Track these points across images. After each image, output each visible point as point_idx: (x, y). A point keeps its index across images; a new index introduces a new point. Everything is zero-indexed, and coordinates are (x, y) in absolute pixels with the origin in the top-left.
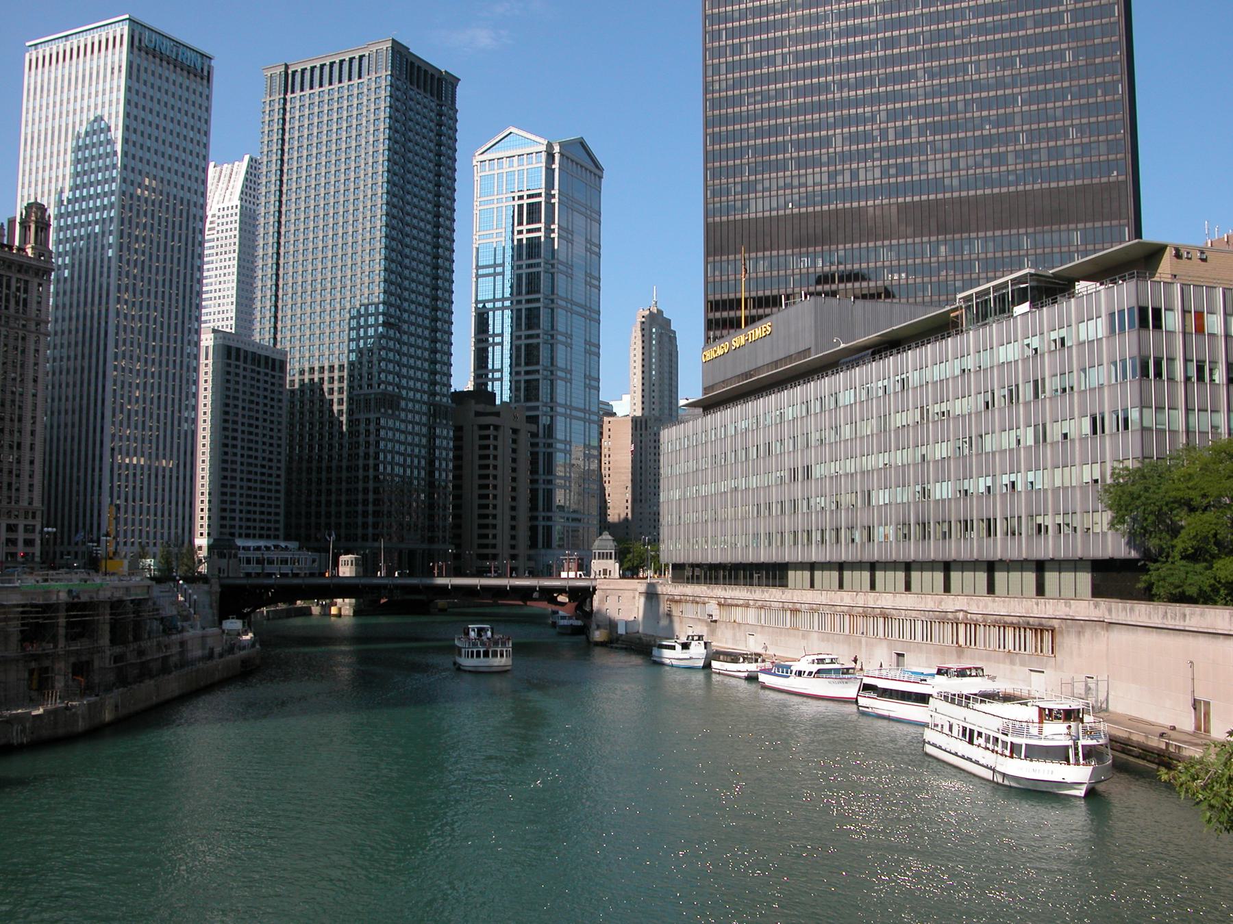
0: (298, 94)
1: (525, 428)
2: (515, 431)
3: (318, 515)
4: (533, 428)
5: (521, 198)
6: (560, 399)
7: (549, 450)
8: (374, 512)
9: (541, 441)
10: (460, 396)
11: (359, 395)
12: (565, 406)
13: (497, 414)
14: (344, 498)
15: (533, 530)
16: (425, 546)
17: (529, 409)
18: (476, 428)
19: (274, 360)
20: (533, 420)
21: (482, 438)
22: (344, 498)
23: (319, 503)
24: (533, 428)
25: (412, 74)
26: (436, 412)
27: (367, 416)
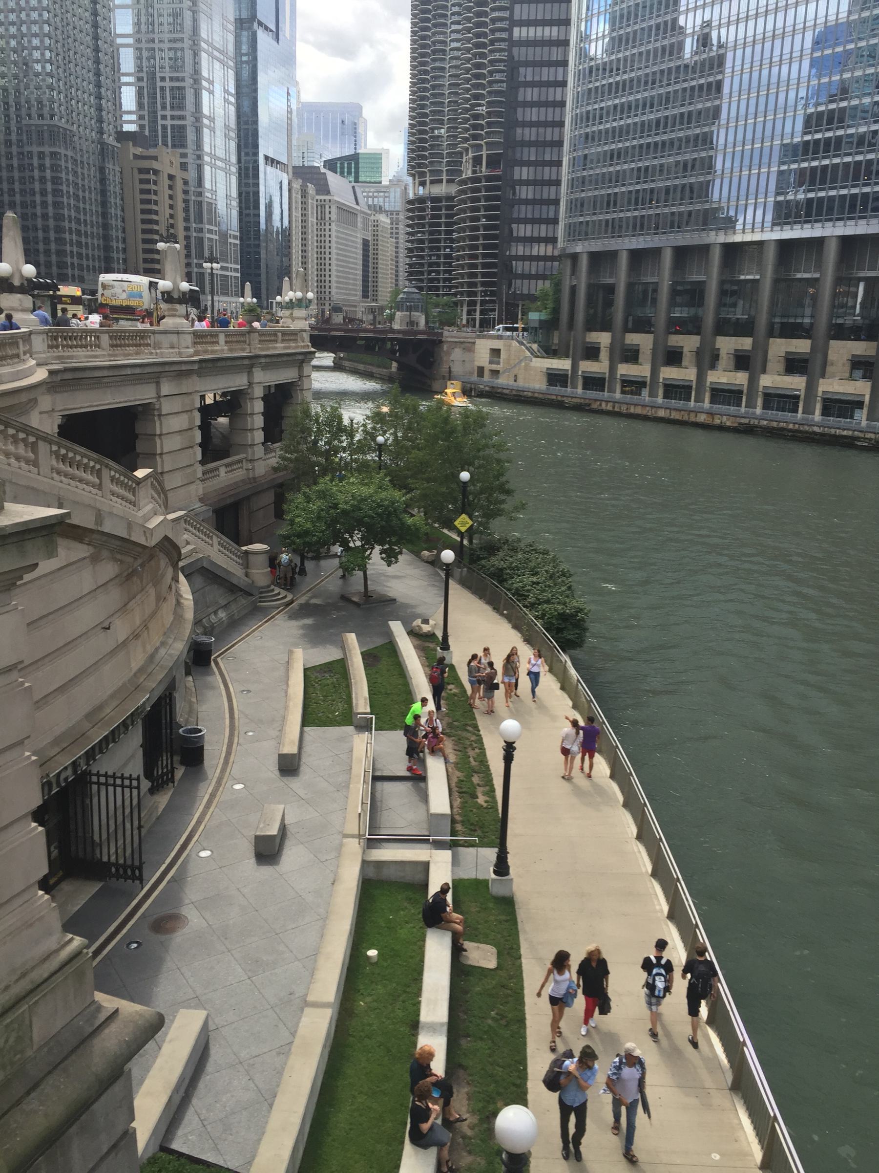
2: (171, 177)
4: (184, 175)
6: (207, 148)
7: (199, 199)
10: (123, 136)
18: (136, 171)
20: (184, 167)
21: (142, 181)
26: (104, 151)
27: (42, 149)
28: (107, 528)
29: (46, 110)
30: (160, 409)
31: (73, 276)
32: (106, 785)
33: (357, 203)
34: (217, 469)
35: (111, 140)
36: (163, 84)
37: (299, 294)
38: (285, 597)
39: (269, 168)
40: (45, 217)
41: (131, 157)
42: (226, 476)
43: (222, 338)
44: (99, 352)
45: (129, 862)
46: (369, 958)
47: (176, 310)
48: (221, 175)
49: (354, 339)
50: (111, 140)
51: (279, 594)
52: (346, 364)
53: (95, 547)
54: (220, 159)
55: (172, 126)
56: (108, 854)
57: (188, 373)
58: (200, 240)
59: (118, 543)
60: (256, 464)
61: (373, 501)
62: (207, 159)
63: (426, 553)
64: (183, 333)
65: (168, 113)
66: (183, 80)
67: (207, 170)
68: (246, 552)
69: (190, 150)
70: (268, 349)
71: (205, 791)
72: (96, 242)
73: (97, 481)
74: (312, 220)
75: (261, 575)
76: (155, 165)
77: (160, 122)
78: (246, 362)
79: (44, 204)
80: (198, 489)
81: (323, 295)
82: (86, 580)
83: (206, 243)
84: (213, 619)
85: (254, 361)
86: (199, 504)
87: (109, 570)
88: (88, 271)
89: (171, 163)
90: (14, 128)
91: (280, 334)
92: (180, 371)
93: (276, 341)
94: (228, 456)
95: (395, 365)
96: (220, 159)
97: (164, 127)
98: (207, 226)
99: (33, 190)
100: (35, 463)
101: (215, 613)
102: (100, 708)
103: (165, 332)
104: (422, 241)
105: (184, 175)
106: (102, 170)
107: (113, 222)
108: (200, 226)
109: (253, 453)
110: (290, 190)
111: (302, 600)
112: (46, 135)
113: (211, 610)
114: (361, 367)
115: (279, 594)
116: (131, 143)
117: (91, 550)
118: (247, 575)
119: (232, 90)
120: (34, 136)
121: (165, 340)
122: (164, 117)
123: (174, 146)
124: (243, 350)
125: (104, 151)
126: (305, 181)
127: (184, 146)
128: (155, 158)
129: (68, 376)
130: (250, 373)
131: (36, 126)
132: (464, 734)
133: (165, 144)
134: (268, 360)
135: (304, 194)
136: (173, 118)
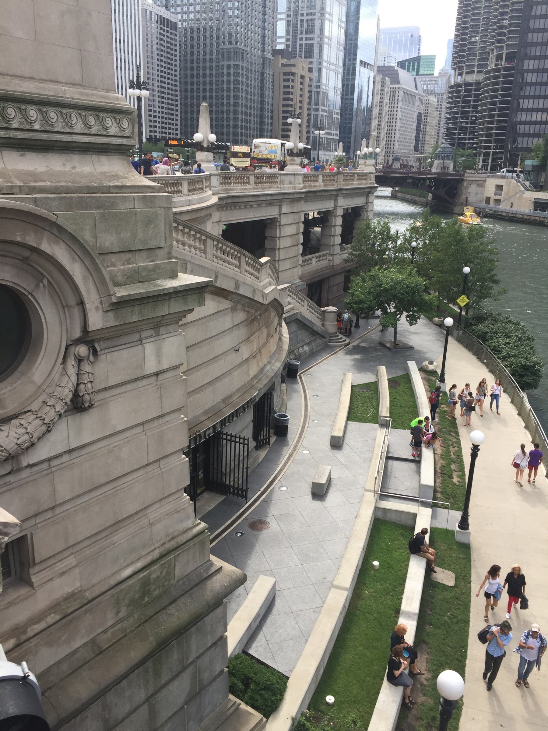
2: (302, 77)
4: (310, 75)
6: (325, 57)
7: (318, 90)
10: (276, 52)
11: (223, 49)
12: (327, 62)
18: (282, 74)
19: (171, 22)
20: (310, 70)
21: (285, 80)
26: (264, 62)
27: (229, 63)
28: (241, 291)
29: (233, 40)
30: (280, 222)
31: (241, 140)
32: (231, 441)
33: (417, 89)
34: (311, 259)
35: (269, 55)
36: (302, 18)
37: (371, 150)
38: (345, 341)
39: (362, 69)
40: (228, 104)
41: (280, 65)
42: (316, 264)
43: (320, 178)
44: (248, 186)
45: (240, 487)
46: (373, 566)
47: (294, 161)
48: (332, 74)
49: (406, 178)
50: (269, 55)
51: (341, 338)
52: (399, 195)
53: (234, 302)
54: (333, 64)
55: (306, 44)
56: (230, 480)
57: (298, 200)
58: (317, 116)
59: (248, 301)
60: (335, 257)
61: (404, 284)
62: (325, 64)
63: (436, 319)
64: (297, 175)
66: (314, 14)
67: (324, 71)
68: (324, 311)
69: (315, 59)
70: (348, 185)
71: (286, 452)
73: (238, 263)
74: (386, 101)
75: (331, 326)
76: (293, 70)
77: (299, 42)
78: (334, 193)
79: (228, 97)
80: (299, 271)
81: (389, 150)
82: (227, 321)
83: (320, 118)
84: (301, 350)
85: (339, 192)
86: (299, 280)
87: (241, 316)
89: (303, 68)
90: (215, 51)
91: (356, 175)
92: (293, 198)
93: (353, 180)
94: (318, 252)
95: (430, 195)
96: (333, 64)
97: (301, 45)
98: (322, 107)
99: (223, 88)
100: (205, 252)
101: (302, 347)
102: (230, 396)
103: (287, 174)
104: (456, 113)
105: (310, 75)
106: (262, 74)
107: (266, 107)
108: (317, 107)
109: (334, 251)
110: (374, 82)
111: (355, 343)
112: (232, 54)
113: (300, 345)
114: (408, 197)
115: (341, 338)
116: (280, 57)
117: (232, 304)
118: (323, 325)
119: (344, 19)
121: (286, 179)
122: (301, 39)
123: (305, 57)
124: (333, 185)
125: (264, 62)
126: (384, 75)
127: (311, 57)
128: (294, 65)
129: (230, 201)
130: (336, 200)
131: (227, 49)
132: (449, 437)
133: (301, 57)
134: (347, 192)
135: (383, 85)
136: (306, 39)
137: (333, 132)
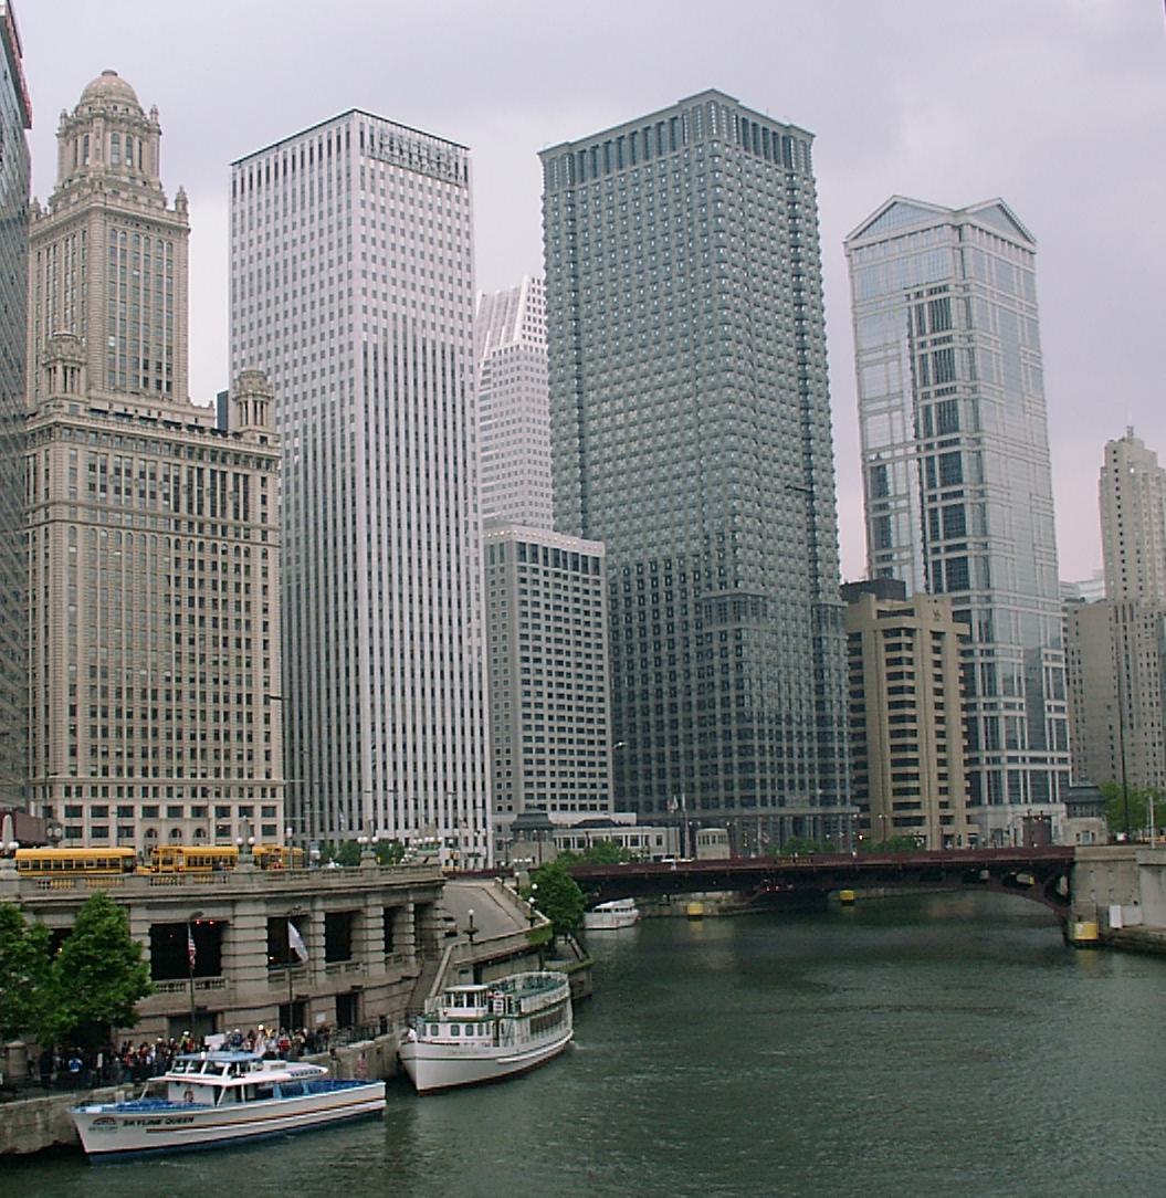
0: (589, 181)
1: (953, 630)
2: (937, 635)
3: (661, 773)
4: (963, 629)
5: (918, 295)
7: (990, 660)
8: (741, 765)
9: (978, 647)
10: (852, 591)
13: (910, 613)
14: (696, 747)
15: (973, 777)
16: (818, 810)
17: (955, 601)
18: (880, 634)
21: (889, 648)
22: (696, 747)
23: (661, 758)
24: (963, 629)
25: (745, 135)
26: (820, 615)
27: (722, 628)
29: (729, 578)
31: (764, 798)
35: (835, 600)
50: (835, 600)
65: (942, 543)
69: (974, 593)
72: (806, 745)
76: (907, 622)
83: (1002, 723)
88: (792, 787)
106: (817, 641)
112: (729, 608)
116: (873, 596)
120: (715, 611)
122: (936, 551)
123: (950, 589)
133: (938, 589)
137: (1048, 754)
